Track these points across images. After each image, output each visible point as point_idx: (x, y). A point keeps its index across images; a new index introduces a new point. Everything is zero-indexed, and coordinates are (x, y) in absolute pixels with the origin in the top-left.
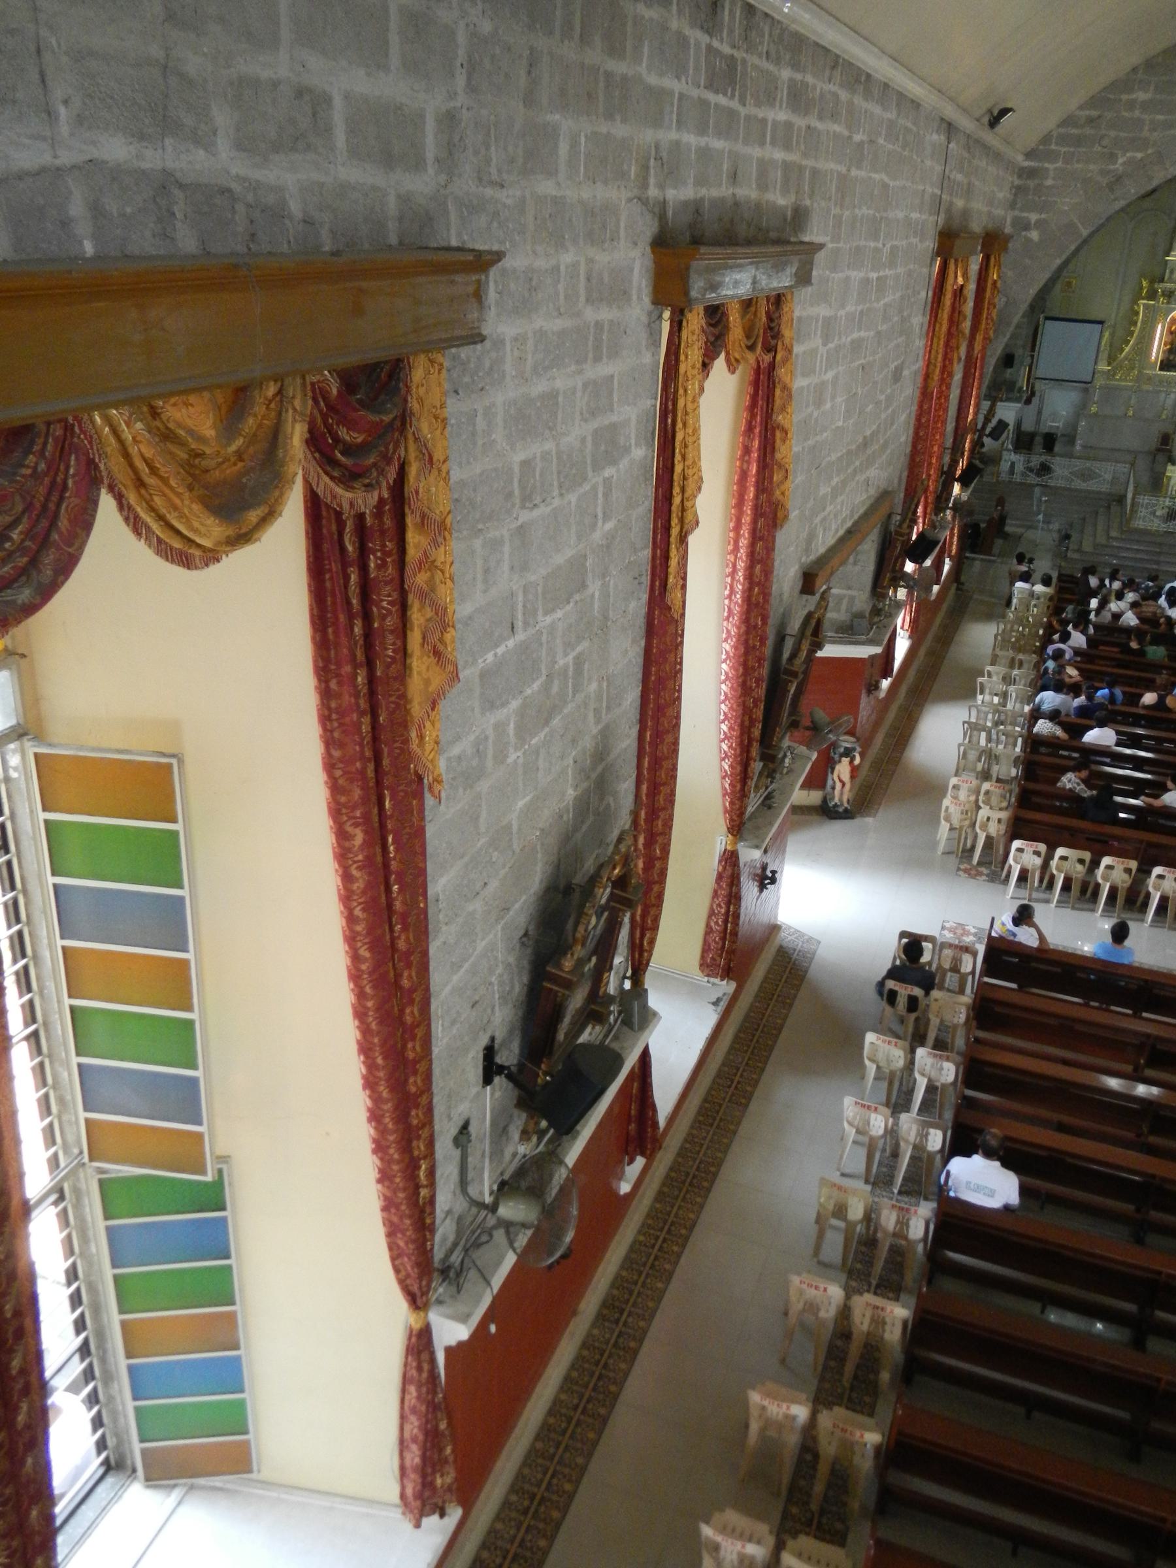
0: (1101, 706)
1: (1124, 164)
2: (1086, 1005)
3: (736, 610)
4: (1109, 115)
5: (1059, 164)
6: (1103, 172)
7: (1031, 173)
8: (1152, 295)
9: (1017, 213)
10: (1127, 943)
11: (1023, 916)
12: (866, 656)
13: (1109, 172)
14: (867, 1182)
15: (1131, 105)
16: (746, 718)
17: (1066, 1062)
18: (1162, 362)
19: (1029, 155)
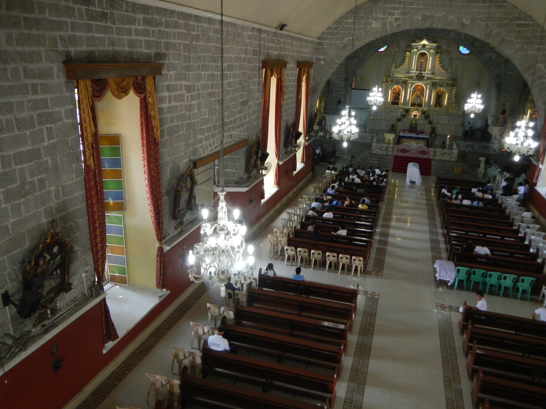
0: (334, 206)
1: (347, 41)
2: (296, 295)
3: (146, 171)
4: (341, 26)
5: (328, 41)
6: (341, 43)
7: (319, 44)
8: (387, 82)
9: (317, 56)
10: (301, 274)
11: (270, 267)
12: (245, 191)
13: (343, 43)
14: (199, 350)
15: (347, 23)
16: (156, 204)
17: (275, 311)
18: (392, 102)
19: (318, 38)
